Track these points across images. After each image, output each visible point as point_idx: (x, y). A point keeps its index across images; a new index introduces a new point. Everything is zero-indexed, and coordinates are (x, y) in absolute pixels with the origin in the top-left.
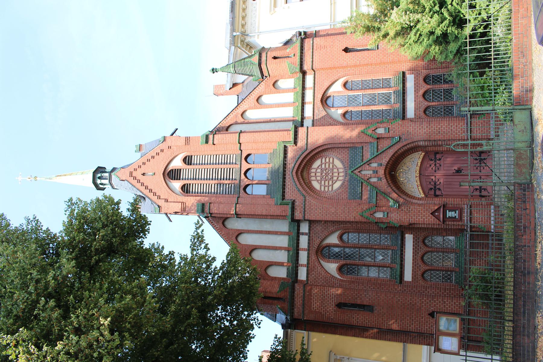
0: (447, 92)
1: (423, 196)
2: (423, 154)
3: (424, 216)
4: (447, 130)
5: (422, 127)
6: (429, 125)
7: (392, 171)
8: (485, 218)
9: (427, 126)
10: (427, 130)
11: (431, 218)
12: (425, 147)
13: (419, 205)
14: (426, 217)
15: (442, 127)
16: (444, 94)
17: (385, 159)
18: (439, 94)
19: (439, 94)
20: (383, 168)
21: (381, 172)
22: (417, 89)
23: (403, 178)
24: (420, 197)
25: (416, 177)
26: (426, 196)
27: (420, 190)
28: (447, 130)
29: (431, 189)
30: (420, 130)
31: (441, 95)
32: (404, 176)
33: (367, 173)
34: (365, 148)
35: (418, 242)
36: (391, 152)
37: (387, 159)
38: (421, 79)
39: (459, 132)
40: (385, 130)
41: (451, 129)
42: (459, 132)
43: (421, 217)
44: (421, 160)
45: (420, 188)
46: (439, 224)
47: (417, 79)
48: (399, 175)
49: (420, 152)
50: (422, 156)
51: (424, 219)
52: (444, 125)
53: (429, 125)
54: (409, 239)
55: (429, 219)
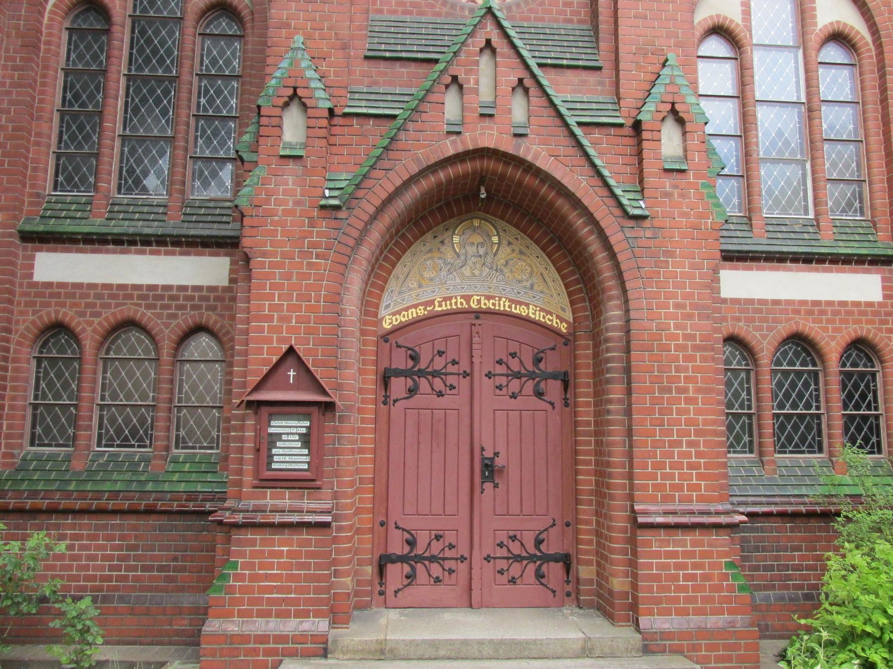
0: (809, 428)
1: (387, 326)
2: (563, 328)
3: (282, 319)
4: (677, 422)
5: (690, 317)
6: (696, 348)
7: (488, 193)
8: (270, 590)
9: (692, 337)
10: (675, 337)
11: (271, 351)
12: (597, 337)
13: (336, 299)
14: (278, 330)
15: (688, 401)
16: (802, 417)
17: (543, 153)
18: (800, 396)
19: (800, 396)
20: (507, 145)
21: (489, 137)
22: (823, 312)
23: (463, 245)
24: (382, 312)
25: (467, 298)
26: (385, 337)
27: (412, 314)
28: (677, 422)
29: (415, 358)
30: (677, 306)
31: (794, 406)
32: (471, 250)
33: (486, 78)
34: (591, 78)
35: (193, 307)
36: (577, 181)
37: (545, 163)
38: (866, 330)
39: (665, 477)
40: (675, 160)
41: (679, 444)
42: (665, 477)
43: (278, 308)
44: (539, 316)
45: (421, 312)
46: (244, 385)
47: (864, 313)
48: (474, 229)
49: (569, 316)
50: (555, 322)
51: (270, 318)
52: (698, 412)
53: (696, 348)
54: (206, 271)
55: (269, 340)
